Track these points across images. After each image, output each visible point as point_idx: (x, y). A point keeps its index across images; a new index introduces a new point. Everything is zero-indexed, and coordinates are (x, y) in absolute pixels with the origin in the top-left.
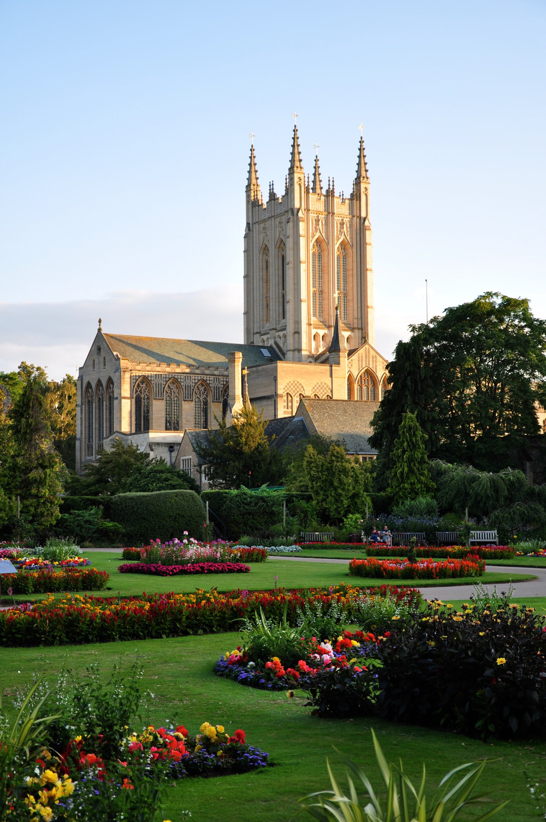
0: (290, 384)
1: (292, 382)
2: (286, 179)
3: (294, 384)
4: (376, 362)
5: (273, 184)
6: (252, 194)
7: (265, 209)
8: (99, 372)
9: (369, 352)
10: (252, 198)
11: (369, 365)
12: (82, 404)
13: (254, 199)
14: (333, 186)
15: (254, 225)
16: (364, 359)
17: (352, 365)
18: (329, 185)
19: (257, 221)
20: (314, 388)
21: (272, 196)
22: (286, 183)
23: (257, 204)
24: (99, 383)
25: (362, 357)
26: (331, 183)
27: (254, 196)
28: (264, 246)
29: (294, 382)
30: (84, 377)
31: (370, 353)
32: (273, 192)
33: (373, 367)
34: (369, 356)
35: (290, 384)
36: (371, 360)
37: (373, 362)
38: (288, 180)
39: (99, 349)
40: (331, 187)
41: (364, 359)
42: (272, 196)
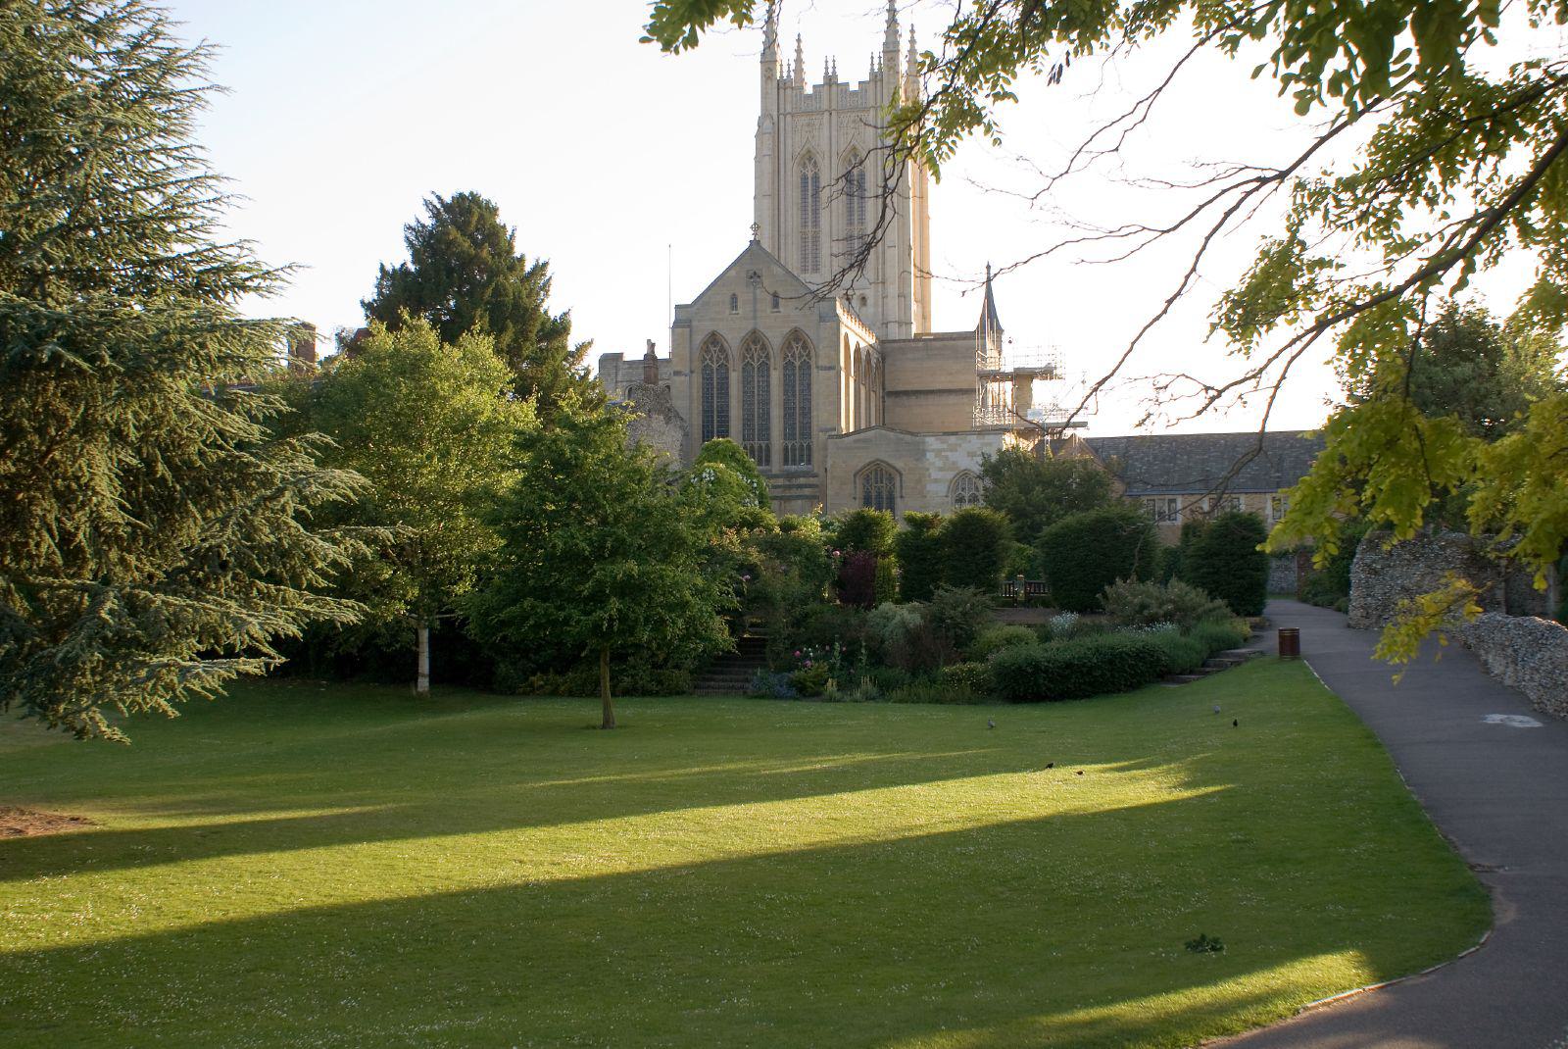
6: (778, 68)
7: (809, 96)
8: (755, 318)
10: (778, 75)
12: (692, 372)
13: (782, 76)
19: (789, 110)
21: (830, 80)
22: (872, 64)
24: (755, 339)
27: (781, 72)
28: (804, 152)
30: (695, 323)
32: (834, 72)
38: (876, 61)
39: (755, 276)
42: (830, 80)
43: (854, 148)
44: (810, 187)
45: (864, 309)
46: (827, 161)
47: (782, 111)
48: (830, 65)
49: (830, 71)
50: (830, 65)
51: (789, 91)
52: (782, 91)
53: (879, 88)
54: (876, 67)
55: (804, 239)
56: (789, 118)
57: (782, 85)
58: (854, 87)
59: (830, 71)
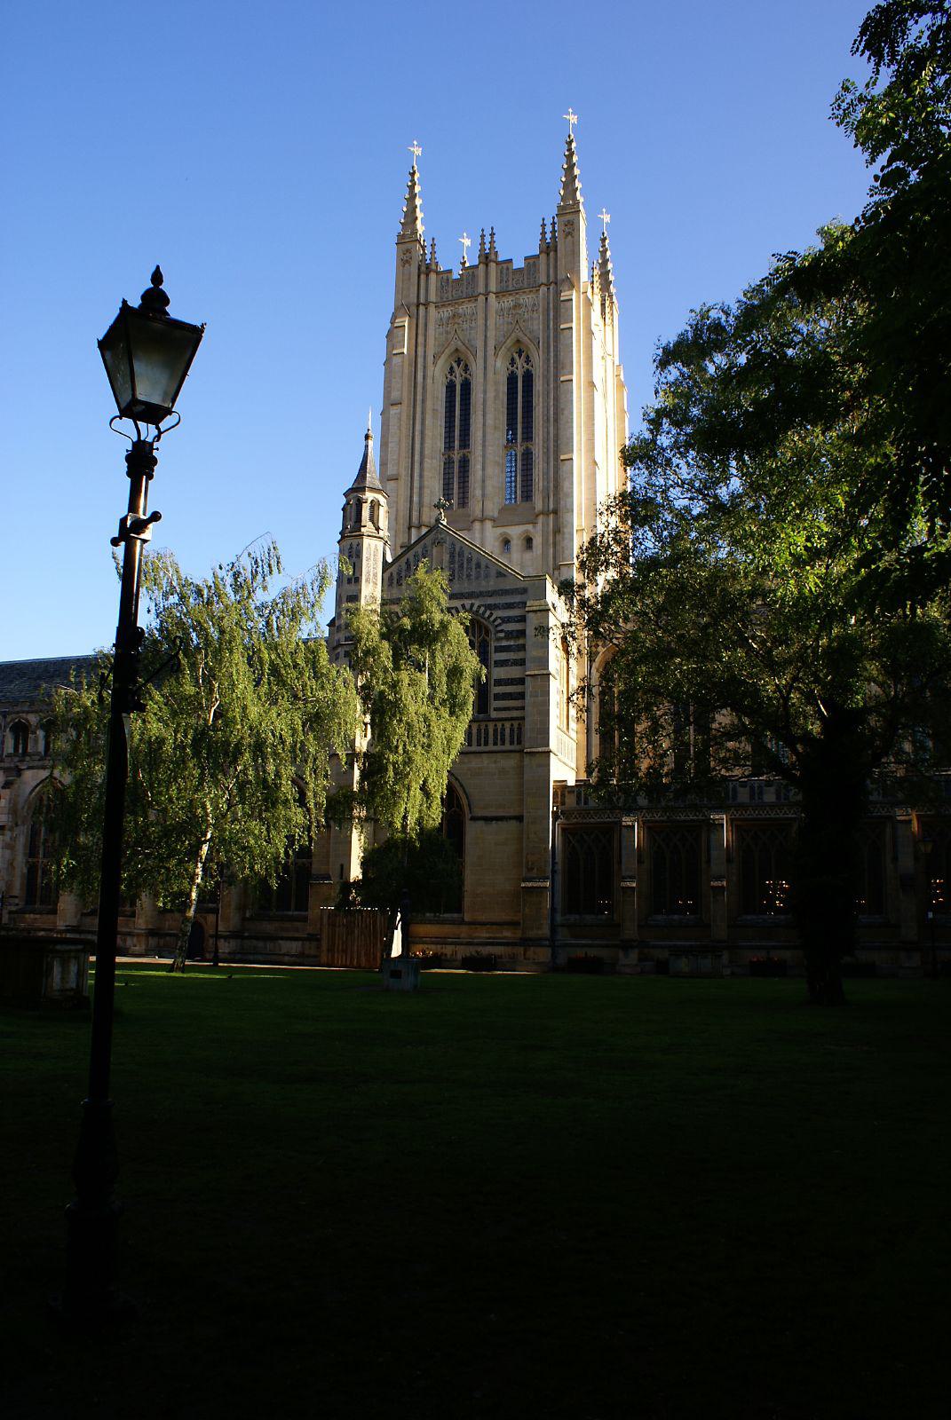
2: (544, 225)
5: (492, 235)
15: (422, 308)
22: (543, 233)
23: (433, 267)
38: (549, 229)
43: (518, 341)
44: (459, 399)
45: (528, 555)
46: (480, 354)
47: (422, 300)
48: (487, 239)
49: (487, 246)
50: (487, 239)
51: (433, 276)
52: (423, 277)
53: (552, 260)
54: (548, 236)
55: (448, 463)
56: (432, 309)
57: (426, 269)
58: (519, 263)
59: (487, 246)
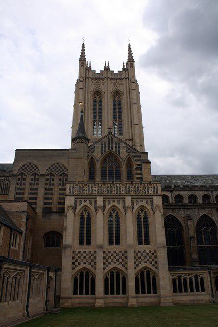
0: (26, 166)
1: (28, 164)
3: (29, 166)
4: (119, 147)
9: (112, 140)
11: (112, 149)
14: (108, 65)
16: (107, 145)
17: (94, 150)
18: (105, 65)
20: (49, 168)
25: (105, 144)
26: (107, 64)
29: (30, 164)
31: (114, 140)
33: (116, 151)
34: (112, 143)
35: (26, 166)
36: (114, 145)
37: (116, 147)
40: (107, 66)
41: (107, 145)
